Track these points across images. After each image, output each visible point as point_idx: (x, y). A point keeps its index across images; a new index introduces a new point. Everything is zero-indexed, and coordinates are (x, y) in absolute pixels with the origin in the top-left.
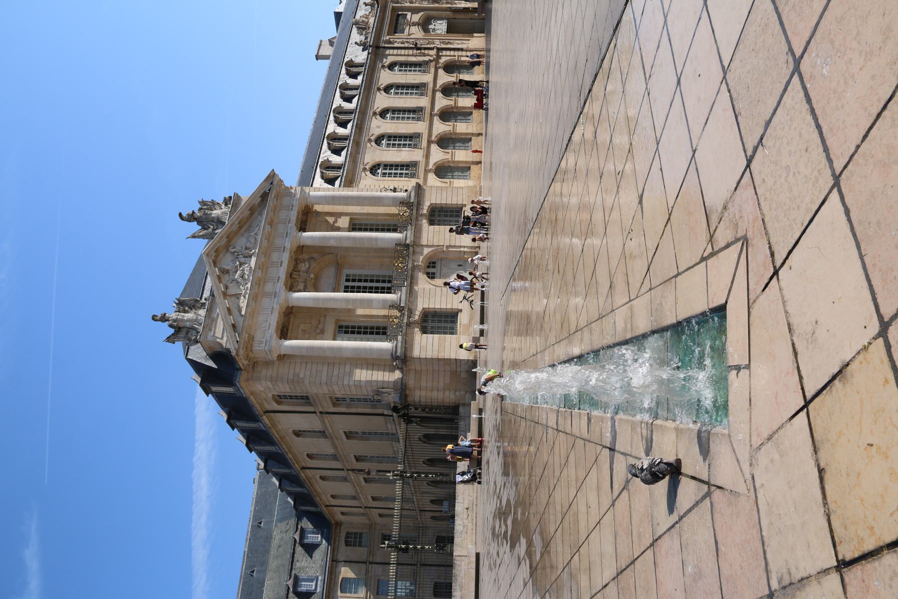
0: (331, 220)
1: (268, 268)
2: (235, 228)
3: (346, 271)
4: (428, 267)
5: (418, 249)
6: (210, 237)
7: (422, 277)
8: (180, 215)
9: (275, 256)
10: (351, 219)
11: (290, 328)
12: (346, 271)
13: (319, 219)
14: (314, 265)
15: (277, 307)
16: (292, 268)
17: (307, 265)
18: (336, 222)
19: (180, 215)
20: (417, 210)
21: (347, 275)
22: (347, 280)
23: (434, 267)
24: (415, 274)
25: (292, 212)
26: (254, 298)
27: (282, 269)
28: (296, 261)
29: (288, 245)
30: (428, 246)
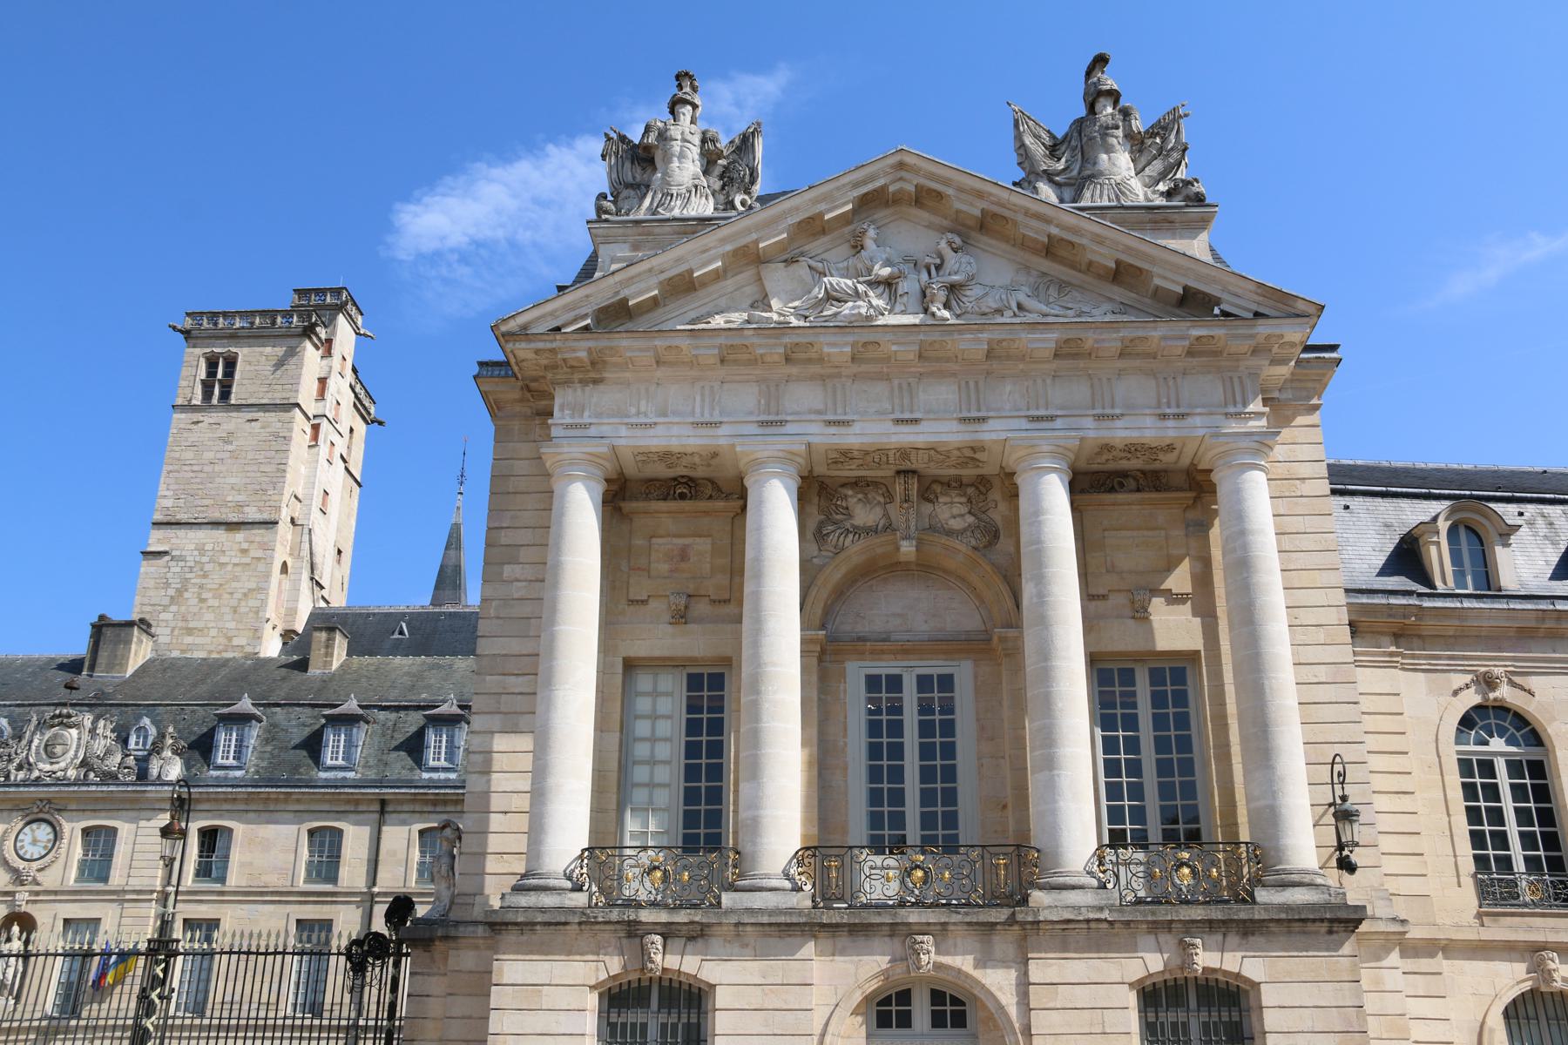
0: (1180, 579)
1: (887, 378)
2: (1036, 231)
3: (964, 673)
4: (937, 997)
5: (1004, 943)
6: (1031, 175)
7: (866, 969)
8: (1101, 61)
9: (943, 394)
10: (1193, 656)
11: (686, 505)
12: (964, 673)
13: (1178, 532)
14: (962, 546)
15: (721, 438)
16: (934, 470)
17: (956, 524)
18: (1174, 599)
19: (1101, 61)
20: (1210, 925)
21: (947, 682)
22: (924, 682)
23: (938, 1021)
24: (877, 943)
25: (1149, 421)
26: (734, 354)
27: (889, 427)
28: (918, 479)
29: (992, 432)
30: (1024, 986)
